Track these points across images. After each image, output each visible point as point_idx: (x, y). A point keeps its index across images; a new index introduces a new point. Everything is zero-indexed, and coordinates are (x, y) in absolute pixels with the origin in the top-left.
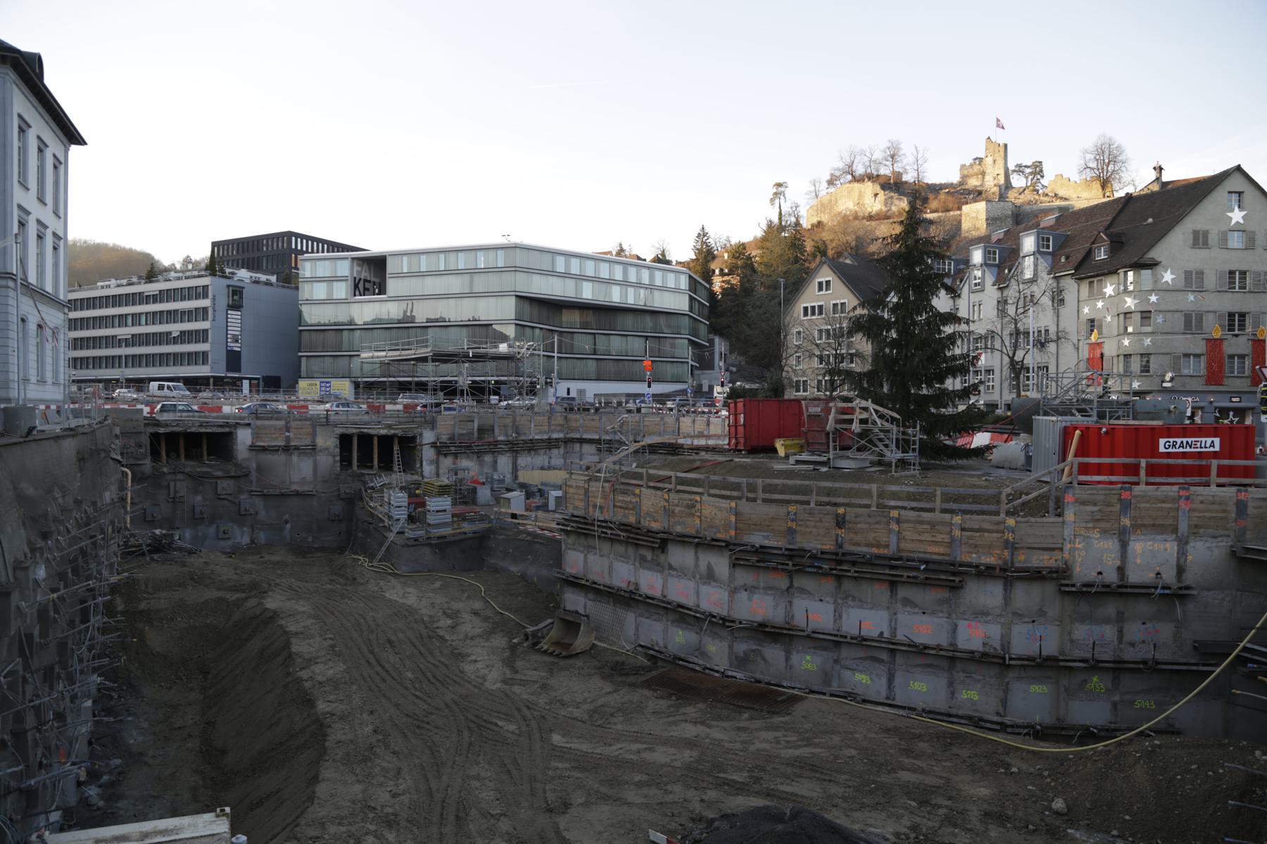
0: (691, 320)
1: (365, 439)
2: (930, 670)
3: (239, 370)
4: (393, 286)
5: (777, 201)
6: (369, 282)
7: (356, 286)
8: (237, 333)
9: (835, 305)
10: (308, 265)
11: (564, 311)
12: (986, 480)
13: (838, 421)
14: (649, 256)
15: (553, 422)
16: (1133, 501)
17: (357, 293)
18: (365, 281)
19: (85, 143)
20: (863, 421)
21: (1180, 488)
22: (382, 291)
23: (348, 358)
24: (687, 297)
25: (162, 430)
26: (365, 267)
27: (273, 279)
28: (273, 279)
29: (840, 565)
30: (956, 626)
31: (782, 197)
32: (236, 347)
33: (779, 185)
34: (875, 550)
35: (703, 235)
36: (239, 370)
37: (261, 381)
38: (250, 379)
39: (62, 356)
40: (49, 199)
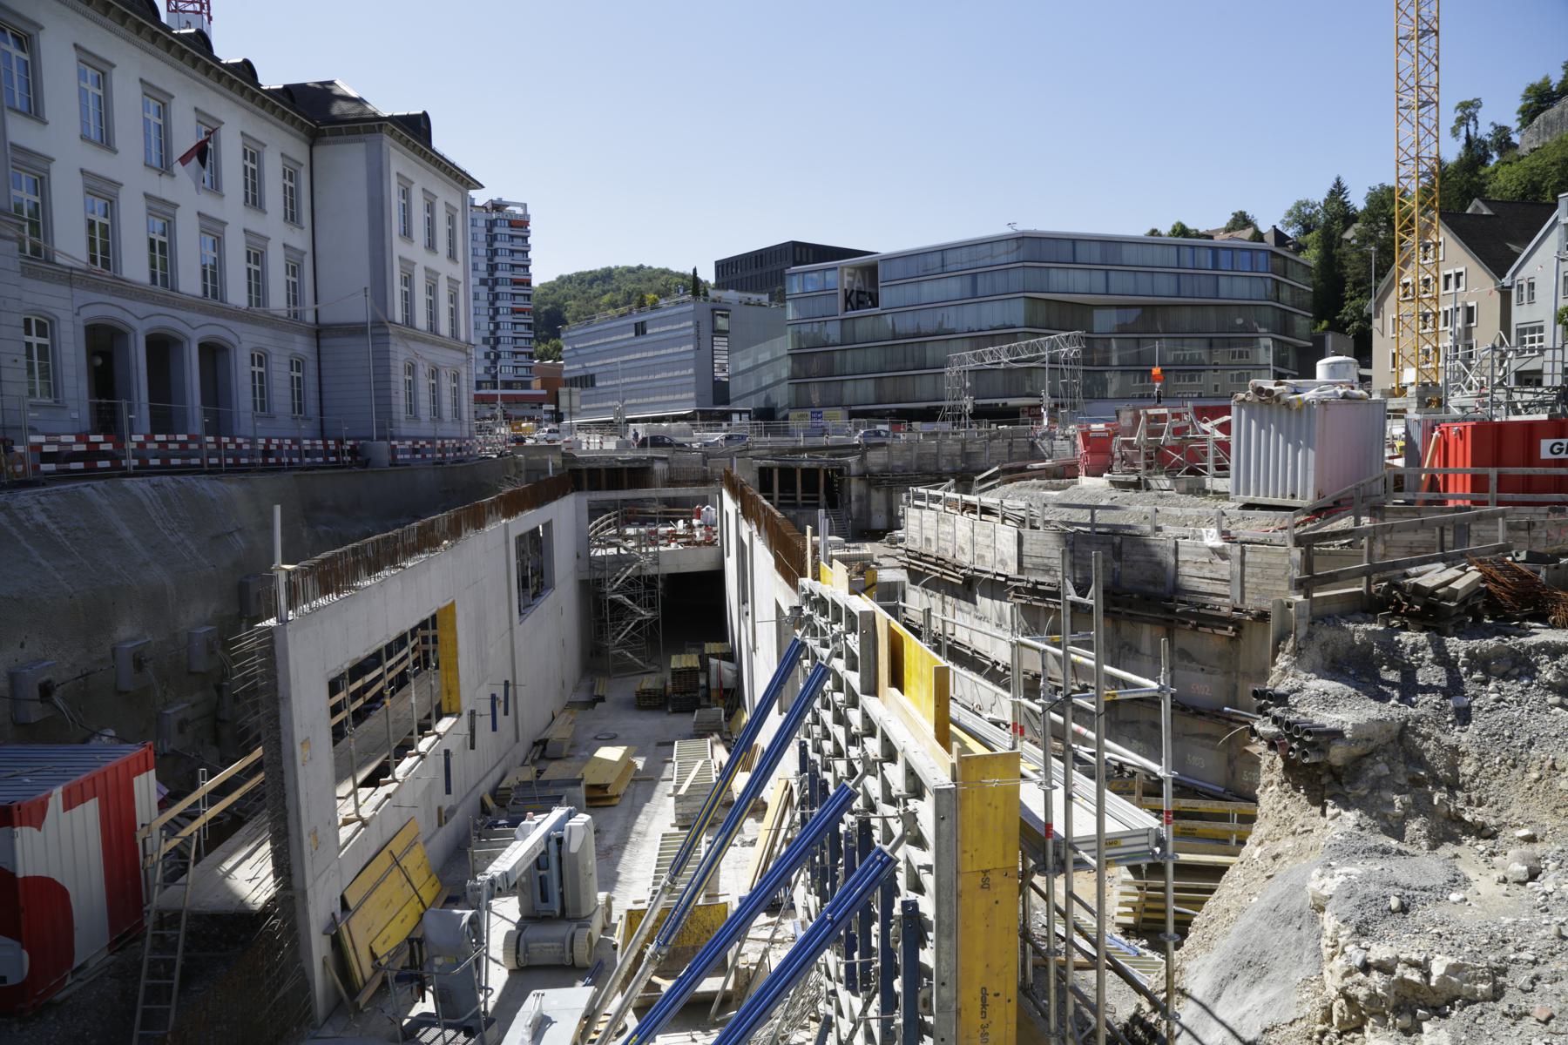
0: (1278, 312)
1: (787, 474)
2: (1207, 741)
4: (886, 296)
5: (1463, 130)
6: (864, 293)
7: (847, 300)
9: (1447, 277)
10: (795, 279)
11: (1095, 311)
13: (1151, 433)
14: (1165, 229)
15: (1015, 450)
16: (1473, 527)
18: (859, 292)
19: (482, 187)
20: (1177, 431)
21: (1550, 510)
22: (875, 305)
24: (1269, 282)
25: (580, 466)
26: (859, 274)
27: (765, 298)
28: (765, 298)
29: (1116, 606)
30: (1236, 687)
31: (1471, 123)
33: (1464, 106)
34: (1151, 588)
35: (1338, 191)
36: (727, 402)
38: (740, 412)
39: (465, 396)
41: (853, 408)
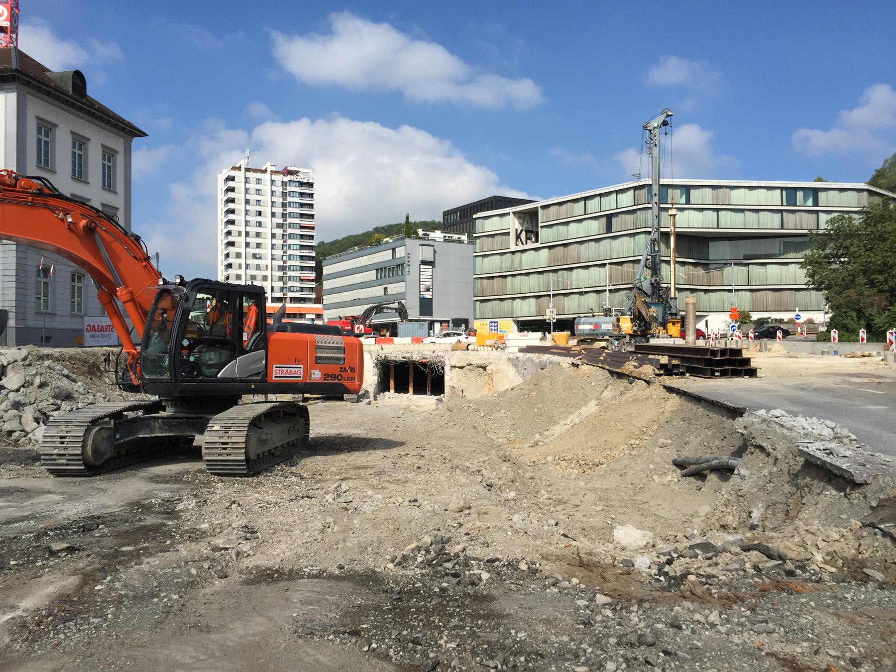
3: (431, 314)
8: (429, 284)
12: (49, 367)
17: (519, 243)
23: (510, 301)
28: (464, 238)
32: (428, 295)
36: (431, 314)
37: (451, 323)
38: (441, 322)
40: (120, 186)
41: (520, 319)
